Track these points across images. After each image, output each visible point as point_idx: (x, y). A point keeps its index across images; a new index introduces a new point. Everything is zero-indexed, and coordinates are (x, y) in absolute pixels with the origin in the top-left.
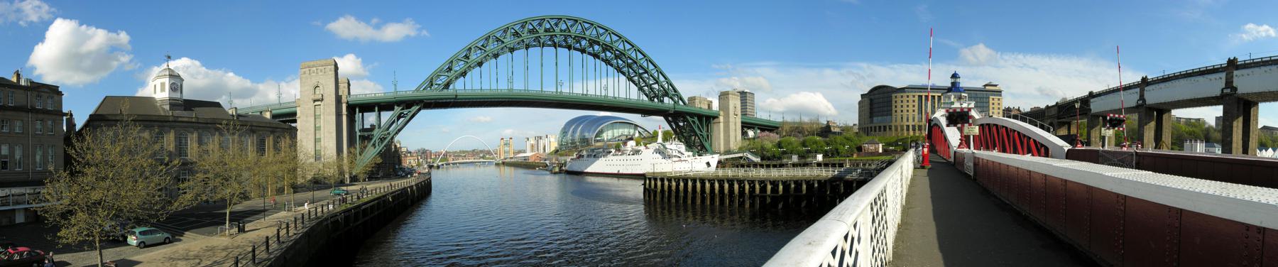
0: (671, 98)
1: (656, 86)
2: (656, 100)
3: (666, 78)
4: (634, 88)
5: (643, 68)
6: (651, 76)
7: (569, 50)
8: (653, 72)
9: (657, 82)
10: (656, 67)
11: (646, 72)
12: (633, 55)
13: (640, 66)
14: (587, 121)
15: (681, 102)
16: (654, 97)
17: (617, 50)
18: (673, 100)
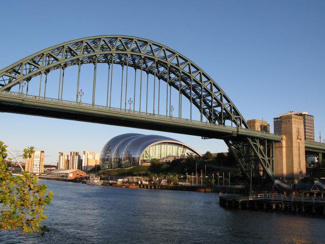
0: (234, 121)
1: (219, 109)
2: (217, 122)
3: (229, 102)
4: (196, 111)
5: (206, 91)
6: (215, 99)
7: (135, 69)
8: (217, 94)
9: (219, 105)
10: (219, 90)
11: (210, 94)
12: (198, 78)
13: (205, 88)
14: (129, 144)
15: (243, 126)
16: (215, 120)
17: (183, 73)
18: (236, 123)
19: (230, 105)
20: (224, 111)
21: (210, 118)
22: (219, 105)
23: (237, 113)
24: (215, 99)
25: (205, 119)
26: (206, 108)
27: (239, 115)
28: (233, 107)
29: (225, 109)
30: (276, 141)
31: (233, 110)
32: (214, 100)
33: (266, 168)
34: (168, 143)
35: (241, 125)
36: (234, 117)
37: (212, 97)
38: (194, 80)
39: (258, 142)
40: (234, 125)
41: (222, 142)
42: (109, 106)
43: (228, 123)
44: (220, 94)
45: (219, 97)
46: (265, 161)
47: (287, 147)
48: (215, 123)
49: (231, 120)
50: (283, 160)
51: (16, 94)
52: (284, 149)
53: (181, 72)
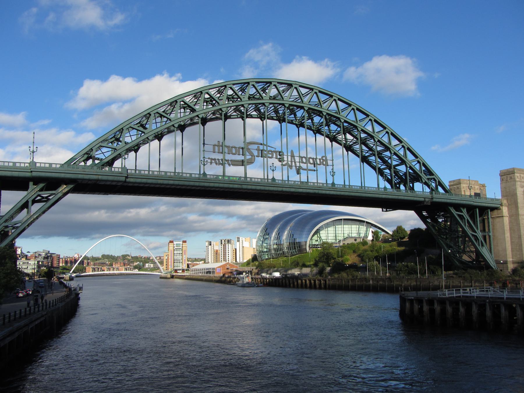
0: (426, 184)
1: (402, 168)
2: (402, 187)
3: (416, 156)
5: (382, 144)
6: (395, 154)
8: (397, 148)
9: (403, 162)
11: (387, 149)
12: (369, 128)
13: (379, 141)
14: (292, 224)
15: (440, 190)
16: (399, 183)
17: (346, 122)
18: (429, 186)
19: (419, 162)
20: (410, 171)
21: (390, 181)
22: (403, 162)
23: (429, 172)
24: (395, 154)
25: (384, 184)
26: (385, 169)
27: (433, 175)
28: (423, 164)
29: (411, 168)
30: (493, 209)
31: (423, 168)
32: (395, 157)
33: (480, 248)
34: (344, 219)
35: (437, 188)
36: (425, 178)
37: (391, 153)
38: (362, 130)
39: (465, 211)
40: (427, 190)
41: (412, 213)
42: (266, 177)
43: (418, 187)
44: (403, 146)
45: (401, 152)
46: (476, 238)
47: (510, 216)
48: (399, 188)
49: (422, 182)
50: (506, 235)
51: (197, 176)
52: (506, 220)
53: (343, 121)
